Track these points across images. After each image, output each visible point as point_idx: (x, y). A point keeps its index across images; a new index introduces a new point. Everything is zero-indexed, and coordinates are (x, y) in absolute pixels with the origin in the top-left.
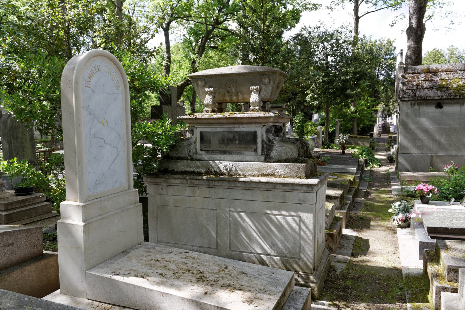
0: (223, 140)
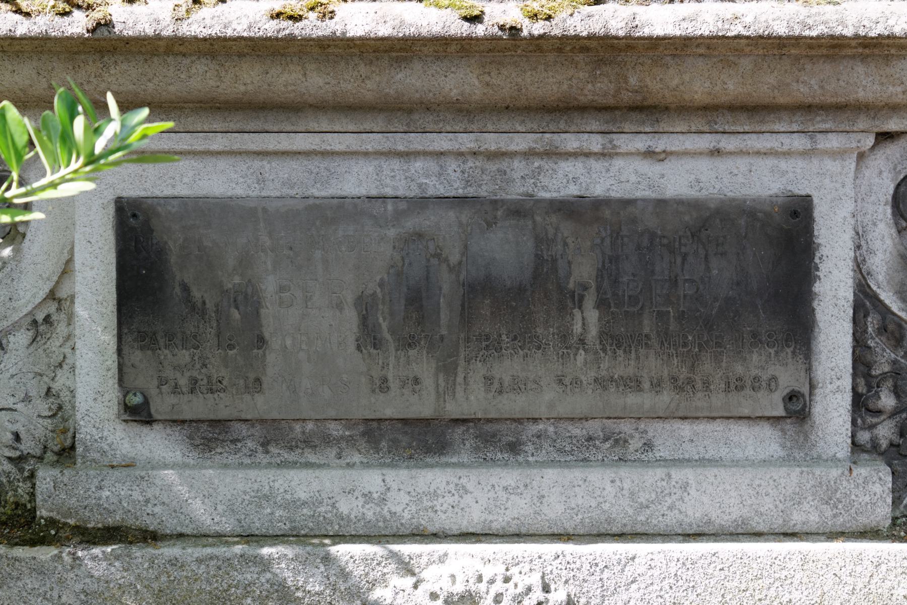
0: (417, 301)
